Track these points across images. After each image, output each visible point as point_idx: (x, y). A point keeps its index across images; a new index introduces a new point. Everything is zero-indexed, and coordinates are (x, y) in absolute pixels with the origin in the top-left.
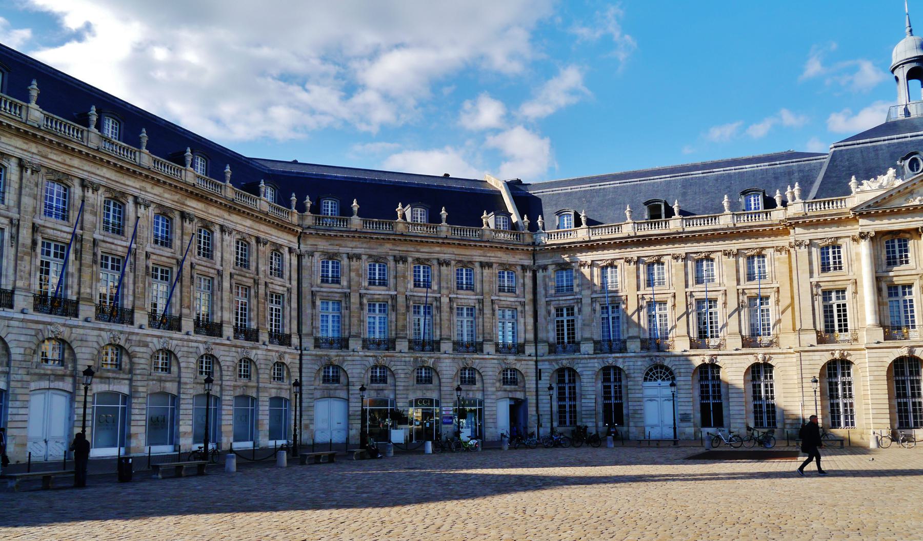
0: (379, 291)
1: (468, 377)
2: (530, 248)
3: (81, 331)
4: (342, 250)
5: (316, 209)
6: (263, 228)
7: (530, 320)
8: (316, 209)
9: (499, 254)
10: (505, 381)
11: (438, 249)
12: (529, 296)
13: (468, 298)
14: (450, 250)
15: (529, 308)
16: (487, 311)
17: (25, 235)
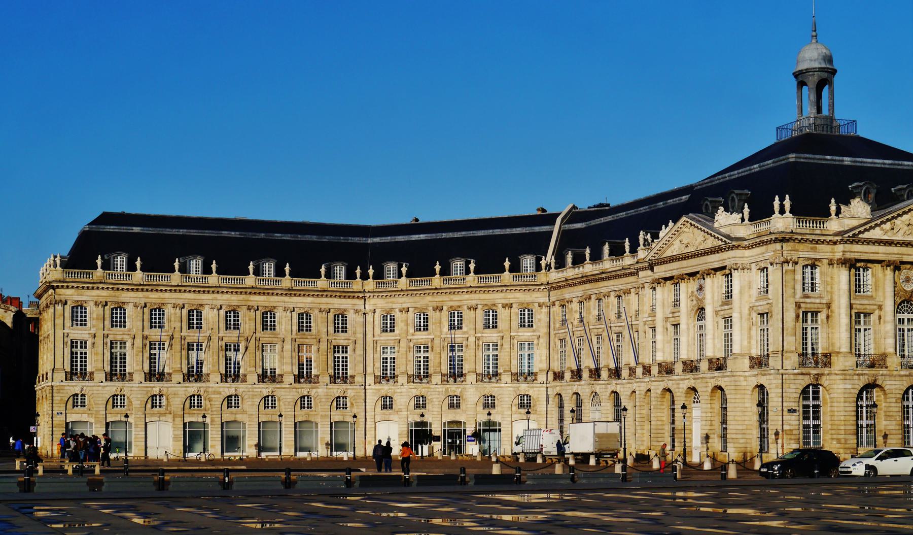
0: (422, 337)
1: (489, 403)
2: (542, 287)
3: (174, 389)
4: (394, 306)
5: (379, 275)
6: (324, 300)
7: (545, 352)
8: (379, 275)
9: (518, 295)
10: (521, 405)
11: (466, 296)
12: (544, 330)
13: (491, 336)
14: (477, 296)
15: (543, 341)
16: (507, 346)
17: (139, 342)
